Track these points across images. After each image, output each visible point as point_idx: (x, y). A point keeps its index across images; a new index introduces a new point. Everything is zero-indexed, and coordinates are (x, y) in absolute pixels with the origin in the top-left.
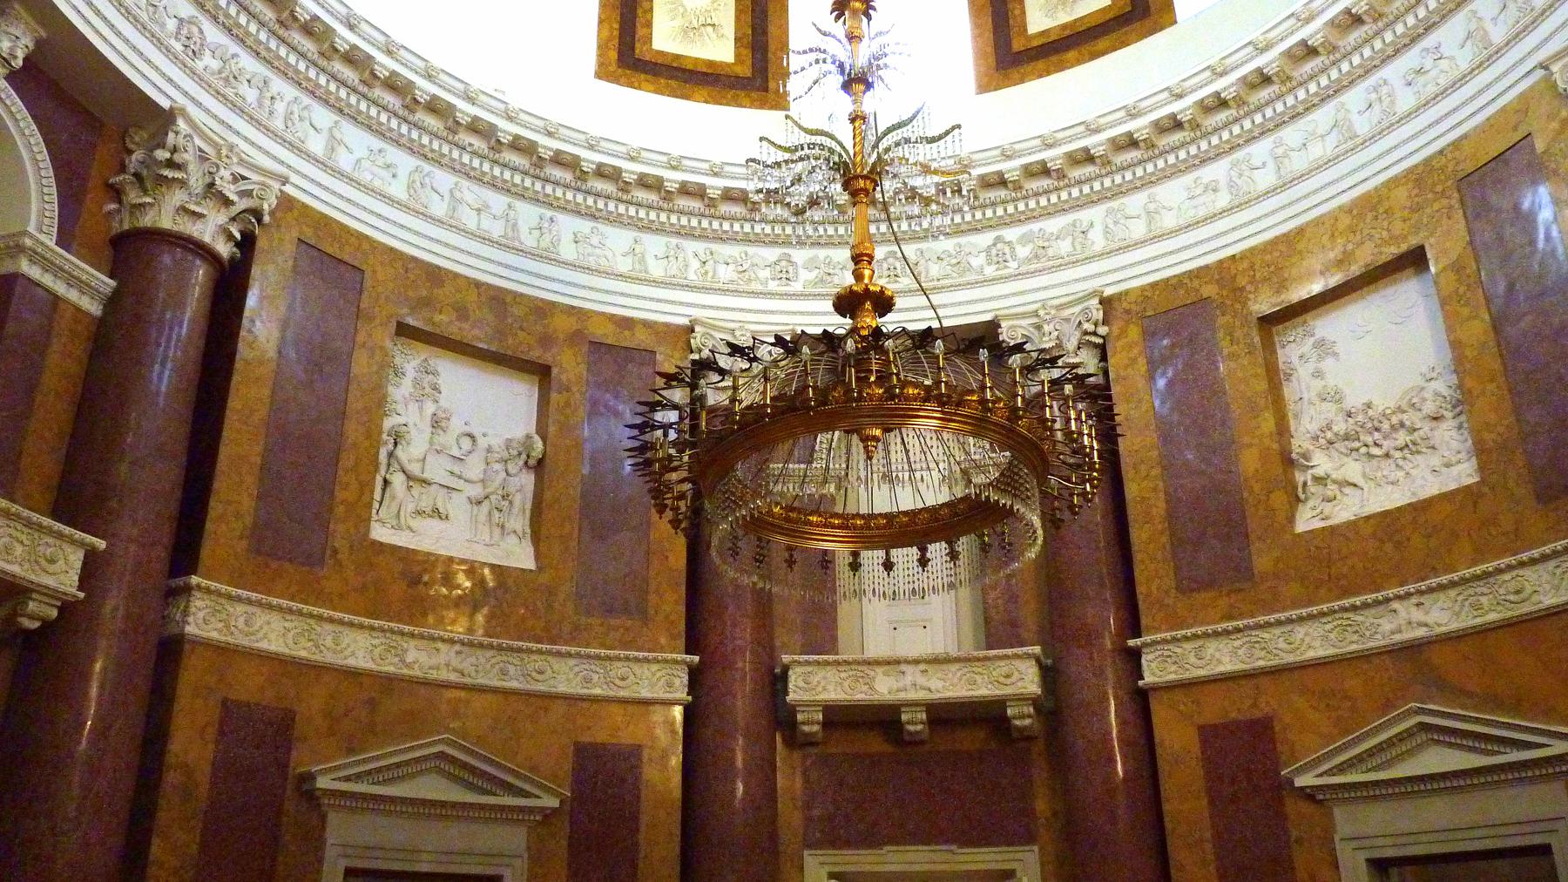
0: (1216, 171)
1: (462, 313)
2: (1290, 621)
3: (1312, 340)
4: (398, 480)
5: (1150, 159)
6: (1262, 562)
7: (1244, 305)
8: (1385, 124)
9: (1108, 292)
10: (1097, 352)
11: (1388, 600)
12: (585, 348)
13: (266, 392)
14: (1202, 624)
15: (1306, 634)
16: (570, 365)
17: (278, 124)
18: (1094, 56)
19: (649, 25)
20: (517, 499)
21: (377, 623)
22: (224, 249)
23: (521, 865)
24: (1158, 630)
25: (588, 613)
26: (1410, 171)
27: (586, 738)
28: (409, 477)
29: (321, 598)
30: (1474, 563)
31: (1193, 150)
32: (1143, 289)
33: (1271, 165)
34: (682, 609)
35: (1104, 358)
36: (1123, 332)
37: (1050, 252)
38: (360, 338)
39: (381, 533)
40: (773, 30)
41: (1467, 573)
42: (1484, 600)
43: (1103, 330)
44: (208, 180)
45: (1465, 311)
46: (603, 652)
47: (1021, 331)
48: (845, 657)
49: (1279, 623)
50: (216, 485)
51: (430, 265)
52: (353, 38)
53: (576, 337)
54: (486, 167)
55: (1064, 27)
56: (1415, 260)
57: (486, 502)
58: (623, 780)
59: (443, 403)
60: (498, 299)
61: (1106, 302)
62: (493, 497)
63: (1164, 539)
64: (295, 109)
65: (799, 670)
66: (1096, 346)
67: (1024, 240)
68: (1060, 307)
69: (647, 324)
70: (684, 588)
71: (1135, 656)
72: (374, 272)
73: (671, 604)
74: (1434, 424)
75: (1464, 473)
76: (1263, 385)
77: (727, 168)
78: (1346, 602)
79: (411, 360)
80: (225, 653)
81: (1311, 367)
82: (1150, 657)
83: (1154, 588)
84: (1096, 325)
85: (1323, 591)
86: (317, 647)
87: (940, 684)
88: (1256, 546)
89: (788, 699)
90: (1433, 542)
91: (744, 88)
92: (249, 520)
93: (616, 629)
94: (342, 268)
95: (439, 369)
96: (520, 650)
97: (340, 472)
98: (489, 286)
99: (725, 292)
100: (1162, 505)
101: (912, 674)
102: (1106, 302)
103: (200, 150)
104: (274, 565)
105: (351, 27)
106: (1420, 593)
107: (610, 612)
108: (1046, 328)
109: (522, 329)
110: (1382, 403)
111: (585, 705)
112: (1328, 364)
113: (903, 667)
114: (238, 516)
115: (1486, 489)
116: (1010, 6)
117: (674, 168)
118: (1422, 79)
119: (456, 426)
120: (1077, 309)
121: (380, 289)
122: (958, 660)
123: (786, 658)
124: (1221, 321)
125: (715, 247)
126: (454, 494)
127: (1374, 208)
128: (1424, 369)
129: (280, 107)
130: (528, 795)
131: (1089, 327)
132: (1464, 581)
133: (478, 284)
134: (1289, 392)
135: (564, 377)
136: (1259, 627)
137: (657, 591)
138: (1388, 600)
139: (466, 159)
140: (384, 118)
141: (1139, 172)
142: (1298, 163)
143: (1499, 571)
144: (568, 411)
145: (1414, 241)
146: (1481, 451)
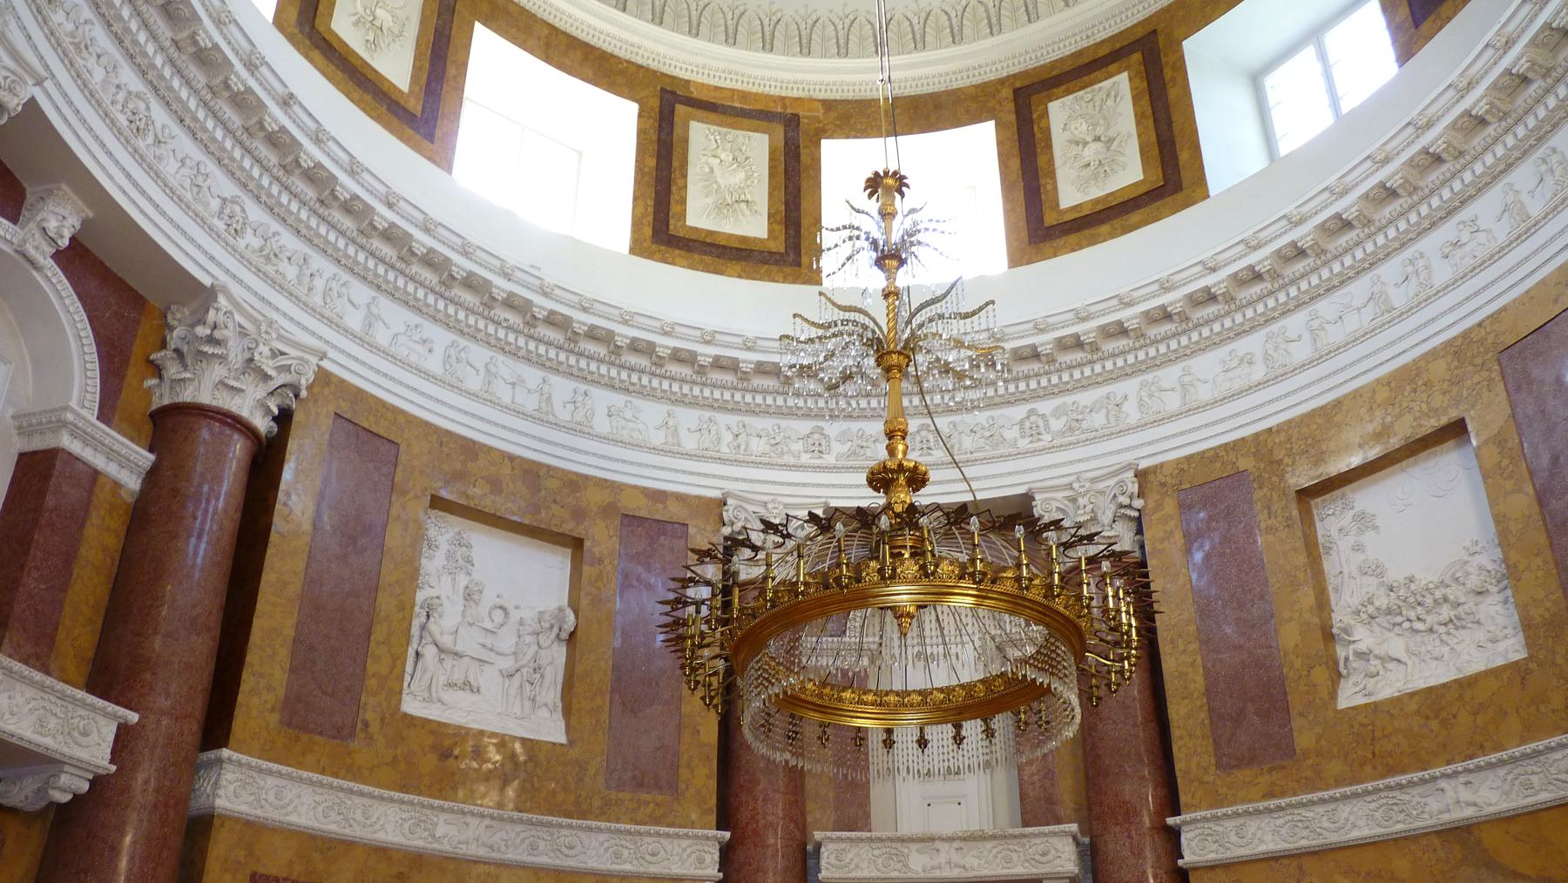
0: (1252, 344)
1: (495, 485)
2: (1334, 799)
3: (1352, 513)
4: (430, 652)
5: (1184, 332)
6: (1304, 739)
7: (1282, 478)
8: (1423, 296)
9: (1143, 465)
10: (1133, 525)
11: (1434, 779)
12: (618, 522)
13: (300, 565)
14: (1243, 801)
15: (1351, 813)
16: (602, 538)
17: (317, 300)
18: (1127, 230)
19: (683, 202)
20: (549, 672)
21: (407, 797)
22: (263, 424)
24: (1197, 808)
25: (620, 787)
26: (1449, 343)
28: (441, 650)
29: (353, 772)
30: (1523, 741)
31: (1228, 323)
32: (1178, 461)
33: (1306, 336)
34: (713, 783)
35: (1140, 531)
36: (1159, 506)
37: (1084, 425)
38: (394, 511)
39: (412, 706)
40: (805, 205)
41: (1517, 751)
42: (1534, 779)
43: (1138, 503)
44: (247, 355)
45: (1509, 485)
46: (633, 827)
47: (1055, 504)
48: (878, 834)
49: (1323, 801)
50: (249, 658)
51: (464, 438)
52: (392, 216)
53: (608, 510)
54: (521, 342)
55: (1097, 201)
56: (1456, 430)
57: (518, 675)
59: (476, 576)
60: (532, 473)
61: (1142, 475)
62: (525, 670)
63: (1203, 715)
64: (334, 285)
65: (831, 846)
66: (1131, 518)
67: (1057, 413)
68: (1094, 480)
69: (680, 497)
70: (715, 762)
71: (1174, 835)
72: (409, 445)
73: (702, 778)
74: (1479, 598)
75: (1512, 649)
76: (1302, 559)
77: (760, 343)
78: (1392, 781)
79: (443, 532)
80: (253, 829)
81: (1351, 539)
82: (1189, 835)
83: (1193, 765)
84: (1131, 498)
85: (1368, 769)
86: (346, 820)
87: (975, 862)
88: (1297, 723)
89: (820, 876)
90: (1481, 720)
91: (776, 263)
92: (281, 693)
93: (647, 803)
94: (379, 442)
97: (372, 644)
99: (757, 464)
100: (1200, 680)
101: (946, 852)
102: (1142, 475)
104: (305, 737)
105: (390, 206)
106: (1468, 771)
107: (638, 788)
108: (1081, 501)
109: (555, 502)
110: (1425, 578)
112: (1369, 538)
113: (938, 844)
114: (270, 688)
115: (1533, 666)
116: (1042, 181)
117: (708, 343)
118: (1459, 252)
119: (489, 598)
120: (1112, 482)
121: (415, 463)
122: (994, 837)
123: (818, 835)
124: (1258, 494)
125: (748, 420)
126: (487, 668)
127: (1413, 381)
128: (1468, 544)
129: (319, 284)
131: (1124, 500)
132: (1514, 760)
133: (512, 458)
134: (1328, 566)
135: (596, 550)
136: (1302, 805)
137: (689, 766)
138: (1434, 779)
139: (501, 333)
140: (421, 293)
141: (1174, 345)
142: (1334, 335)
143: (1550, 749)
144: (600, 584)
145: (1454, 414)
146: (1527, 626)
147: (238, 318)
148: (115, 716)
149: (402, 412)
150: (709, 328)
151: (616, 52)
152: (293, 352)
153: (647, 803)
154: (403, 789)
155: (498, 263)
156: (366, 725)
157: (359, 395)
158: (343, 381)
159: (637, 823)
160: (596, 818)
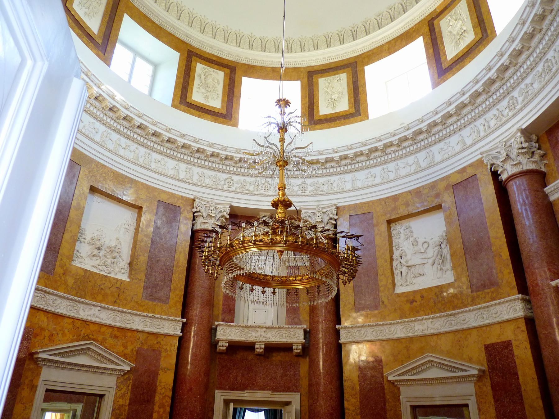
1: (407, 204)
21: (403, 320)
23: (474, 398)
27: (488, 342)
38: (376, 232)
46: (486, 304)
51: (393, 196)
53: (447, 188)
54: (401, 153)
58: (507, 357)
59: (415, 236)
69: (471, 165)
70: (511, 265)
73: (507, 275)
95: (411, 225)
96: (455, 314)
97: (379, 277)
107: (482, 288)
109: (428, 197)
111: (484, 328)
114: (349, 303)
119: (421, 241)
130: (466, 371)
133: (410, 192)
144: (451, 217)
147: (310, 211)
148: (301, 328)
150: (447, 100)
151: (410, 27)
152: (328, 209)
153: (488, 293)
154: (401, 318)
155: (375, 140)
156: (383, 302)
157: (356, 206)
158: (349, 205)
159: (486, 302)
160: (471, 306)
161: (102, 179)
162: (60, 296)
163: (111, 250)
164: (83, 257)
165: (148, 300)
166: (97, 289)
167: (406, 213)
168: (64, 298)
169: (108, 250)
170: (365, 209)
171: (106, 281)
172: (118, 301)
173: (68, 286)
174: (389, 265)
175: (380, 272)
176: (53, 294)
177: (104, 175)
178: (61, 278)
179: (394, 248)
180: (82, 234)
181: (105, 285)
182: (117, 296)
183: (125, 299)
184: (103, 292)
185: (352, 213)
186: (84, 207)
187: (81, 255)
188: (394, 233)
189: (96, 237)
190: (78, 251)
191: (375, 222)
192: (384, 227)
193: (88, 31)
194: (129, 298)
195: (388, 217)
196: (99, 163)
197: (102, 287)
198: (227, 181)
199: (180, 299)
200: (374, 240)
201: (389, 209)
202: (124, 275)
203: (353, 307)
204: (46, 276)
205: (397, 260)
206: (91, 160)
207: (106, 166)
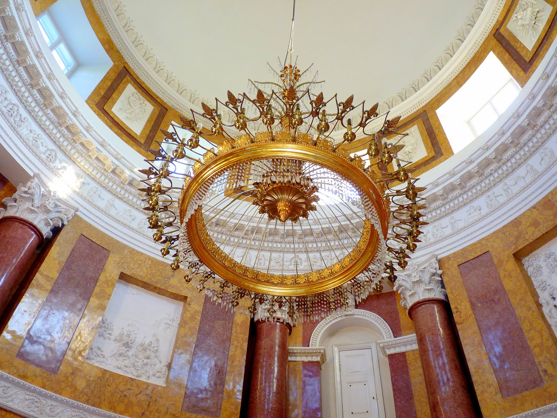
22: (437, 294)
38: (502, 274)
51: (512, 221)
54: (505, 168)
72: (492, 247)
92: (496, 385)
94: (481, 258)
95: (553, 251)
98: (539, 202)
103: (406, 275)
104: (519, 396)
114: (489, 386)
121: (499, 250)
133: (534, 207)
139: (496, 175)
140: (461, 199)
149: (483, 239)
151: (475, 51)
155: (464, 164)
156: (545, 371)
158: (454, 253)
161: (136, 266)
162: (62, 402)
163: (144, 348)
164: (106, 356)
165: (190, 412)
166: (118, 396)
167: (538, 234)
168: (67, 403)
169: (140, 349)
170: (478, 250)
171: (132, 385)
172: (147, 413)
173: (76, 389)
174: (536, 313)
175: (525, 326)
176: (51, 398)
177: (140, 262)
178: (67, 379)
179: (538, 290)
180: (107, 328)
181: (130, 391)
182: (146, 407)
183: (158, 411)
184: (126, 400)
185: (461, 260)
186: (110, 295)
187: (103, 353)
188: (530, 271)
189: (126, 333)
190: (99, 349)
191: (496, 261)
192: (511, 264)
193: (129, 132)
194: (163, 410)
195: (513, 250)
196: (134, 250)
197: (126, 393)
198: (293, 261)
199: (236, 409)
200: (502, 286)
201: (511, 239)
202: (159, 379)
203: (498, 390)
204: (45, 375)
205: (548, 304)
206: (125, 247)
207: (142, 254)
